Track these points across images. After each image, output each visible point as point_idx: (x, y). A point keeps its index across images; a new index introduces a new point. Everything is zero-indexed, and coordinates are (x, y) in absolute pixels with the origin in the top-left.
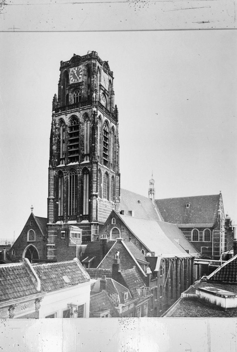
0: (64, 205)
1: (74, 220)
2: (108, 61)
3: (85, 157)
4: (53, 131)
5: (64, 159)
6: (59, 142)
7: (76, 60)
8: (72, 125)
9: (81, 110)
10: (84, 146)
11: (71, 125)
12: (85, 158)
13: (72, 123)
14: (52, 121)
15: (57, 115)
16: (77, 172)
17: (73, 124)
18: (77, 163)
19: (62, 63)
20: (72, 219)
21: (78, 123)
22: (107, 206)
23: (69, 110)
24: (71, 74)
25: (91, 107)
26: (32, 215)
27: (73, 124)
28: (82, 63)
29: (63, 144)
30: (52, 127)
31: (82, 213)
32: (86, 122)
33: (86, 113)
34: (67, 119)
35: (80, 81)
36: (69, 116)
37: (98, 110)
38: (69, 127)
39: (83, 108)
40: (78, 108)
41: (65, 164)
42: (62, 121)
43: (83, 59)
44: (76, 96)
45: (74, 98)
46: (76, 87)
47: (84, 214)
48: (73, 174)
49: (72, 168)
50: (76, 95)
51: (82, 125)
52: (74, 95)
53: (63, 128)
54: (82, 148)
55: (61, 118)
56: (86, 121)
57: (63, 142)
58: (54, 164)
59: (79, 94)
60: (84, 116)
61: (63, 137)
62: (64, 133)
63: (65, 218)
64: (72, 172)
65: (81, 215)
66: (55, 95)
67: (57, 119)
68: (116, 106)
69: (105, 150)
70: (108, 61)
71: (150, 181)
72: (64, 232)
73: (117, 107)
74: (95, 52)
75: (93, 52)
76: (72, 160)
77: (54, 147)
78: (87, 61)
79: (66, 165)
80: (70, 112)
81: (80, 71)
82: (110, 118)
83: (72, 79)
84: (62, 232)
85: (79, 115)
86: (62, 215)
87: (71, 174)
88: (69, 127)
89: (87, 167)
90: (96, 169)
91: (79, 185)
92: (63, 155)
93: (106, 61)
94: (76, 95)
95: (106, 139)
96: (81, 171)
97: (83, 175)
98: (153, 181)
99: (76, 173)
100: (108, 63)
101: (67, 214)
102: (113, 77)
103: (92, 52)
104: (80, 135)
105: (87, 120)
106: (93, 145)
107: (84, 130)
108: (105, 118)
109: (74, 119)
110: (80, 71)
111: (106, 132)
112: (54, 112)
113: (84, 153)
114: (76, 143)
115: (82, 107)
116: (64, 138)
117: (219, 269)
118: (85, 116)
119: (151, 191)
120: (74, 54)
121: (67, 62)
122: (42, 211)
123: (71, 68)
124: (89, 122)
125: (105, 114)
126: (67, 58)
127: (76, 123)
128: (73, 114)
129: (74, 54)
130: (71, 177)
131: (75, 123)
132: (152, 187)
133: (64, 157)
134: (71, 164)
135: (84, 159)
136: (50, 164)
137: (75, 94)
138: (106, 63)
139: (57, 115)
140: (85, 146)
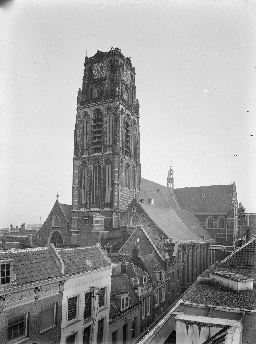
0: (87, 193)
1: (97, 207)
2: (130, 58)
3: (107, 148)
4: (78, 123)
5: (88, 149)
6: (83, 133)
7: (100, 56)
8: (96, 117)
10: (106, 138)
12: (108, 149)
13: (96, 115)
14: (77, 114)
17: (97, 117)
18: (100, 154)
20: (95, 206)
21: (101, 116)
22: (128, 194)
23: (92, 103)
24: (95, 70)
26: (57, 202)
30: (77, 119)
31: (104, 201)
33: (109, 106)
34: (91, 112)
35: (104, 76)
37: (121, 104)
39: (106, 102)
41: (89, 155)
42: (86, 114)
43: (107, 55)
44: (100, 90)
45: (98, 92)
46: (100, 82)
47: (106, 202)
49: (96, 159)
51: (105, 118)
52: (98, 89)
55: (85, 111)
57: (87, 134)
58: (79, 155)
59: (102, 88)
60: (107, 109)
61: (87, 129)
62: (88, 125)
63: (88, 206)
65: (103, 203)
66: (80, 89)
67: (82, 112)
68: (137, 100)
69: (127, 141)
70: (130, 58)
71: (169, 171)
72: (88, 218)
73: (139, 101)
74: (118, 49)
75: (116, 48)
76: (96, 150)
77: (79, 139)
78: (110, 57)
80: (94, 105)
81: (103, 67)
82: (132, 112)
83: (96, 74)
84: (85, 218)
85: (103, 108)
86: (85, 203)
87: (94, 164)
89: (109, 157)
92: (87, 146)
93: (129, 57)
95: (128, 131)
97: (106, 165)
98: (172, 172)
99: (99, 163)
100: (131, 59)
101: (90, 202)
102: (135, 72)
103: (115, 48)
105: (110, 113)
106: (115, 136)
107: (106, 122)
108: (127, 112)
109: (98, 112)
110: (103, 67)
111: (127, 124)
113: (106, 144)
114: (99, 135)
115: (105, 100)
116: (88, 130)
117: (232, 255)
119: (170, 181)
120: (98, 51)
121: (92, 58)
122: (67, 199)
123: (95, 63)
124: (111, 115)
125: (127, 108)
126: (92, 54)
127: (100, 116)
128: (97, 107)
129: (98, 51)
130: (94, 166)
131: (98, 116)
132: (170, 177)
133: (88, 148)
134: (95, 154)
136: (74, 154)
137: (99, 88)
138: (129, 59)
139: (81, 108)
140: (108, 137)
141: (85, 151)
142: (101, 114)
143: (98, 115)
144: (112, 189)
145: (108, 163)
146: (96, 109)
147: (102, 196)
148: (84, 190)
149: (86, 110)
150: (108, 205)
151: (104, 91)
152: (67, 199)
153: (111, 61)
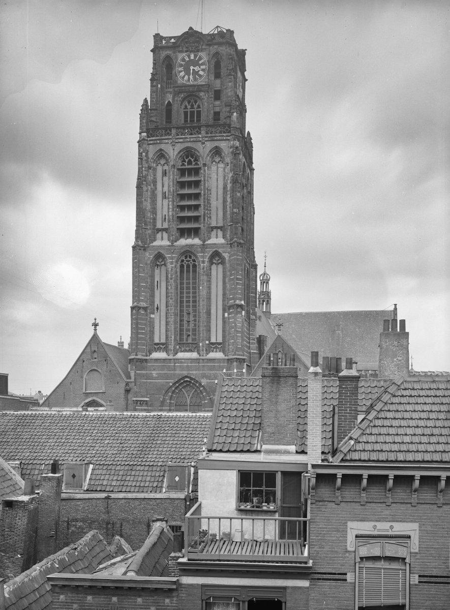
1: (190, 351)
2: (246, 50)
5: (166, 230)
7: (191, 39)
9: (207, 139)
10: (210, 210)
11: (181, 166)
13: (185, 162)
15: (151, 142)
16: (196, 257)
17: (186, 164)
18: (197, 241)
19: (157, 37)
20: (187, 349)
21: (196, 164)
24: (181, 65)
25: (228, 138)
26: (95, 339)
27: (186, 164)
28: (204, 47)
29: (164, 200)
31: (209, 339)
32: (214, 163)
34: (173, 151)
35: (200, 82)
36: (179, 147)
38: (178, 169)
40: (200, 136)
42: (161, 155)
46: (191, 94)
48: (187, 261)
49: (188, 253)
50: (189, 107)
51: (208, 169)
52: (186, 106)
53: (163, 170)
54: (208, 213)
55: (161, 150)
56: (214, 161)
57: (164, 196)
59: (195, 106)
60: (212, 152)
61: (163, 186)
62: (166, 179)
63: (171, 347)
64: (186, 257)
65: (207, 342)
66: (146, 100)
67: (152, 150)
70: (246, 50)
74: (232, 32)
76: (183, 233)
78: (216, 47)
79: (172, 244)
80: (181, 140)
81: (200, 62)
83: (182, 74)
85: (204, 149)
86: (163, 341)
87: (182, 261)
88: (178, 169)
89: (220, 250)
90: (240, 256)
91: (203, 284)
94: (189, 107)
96: (207, 257)
97: (210, 266)
104: (205, 186)
105: (217, 160)
106: (235, 210)
109: (189, 154)
110: (200, 62)
112: (144, 134)
116: (166, 189)
118: (213, 153)
120: (191, 28)
121: (171, 38)
122: (118, 332)
124: (221, 165)
128: (189, 145)
129: (191, 28)
133: (166, 226)
134: (183, 242)
135: (211, 234)
136: (137, 238)
137: (187, 105)
139: (151, 142)
141: (160, 233)
142: (196, 160)
143: (190, 160)
144: (226, 315)
145: (214, 261)
146: (187, 148)
147: (205, 328)
148: (158, 314)
149: (163, 146)
150: (216, 348)
151: (199, 113)
152: (118, 332)
153: (217, 53)
